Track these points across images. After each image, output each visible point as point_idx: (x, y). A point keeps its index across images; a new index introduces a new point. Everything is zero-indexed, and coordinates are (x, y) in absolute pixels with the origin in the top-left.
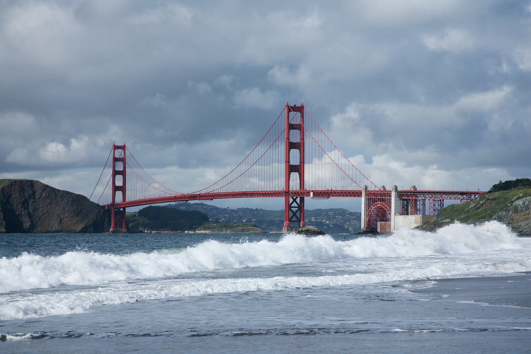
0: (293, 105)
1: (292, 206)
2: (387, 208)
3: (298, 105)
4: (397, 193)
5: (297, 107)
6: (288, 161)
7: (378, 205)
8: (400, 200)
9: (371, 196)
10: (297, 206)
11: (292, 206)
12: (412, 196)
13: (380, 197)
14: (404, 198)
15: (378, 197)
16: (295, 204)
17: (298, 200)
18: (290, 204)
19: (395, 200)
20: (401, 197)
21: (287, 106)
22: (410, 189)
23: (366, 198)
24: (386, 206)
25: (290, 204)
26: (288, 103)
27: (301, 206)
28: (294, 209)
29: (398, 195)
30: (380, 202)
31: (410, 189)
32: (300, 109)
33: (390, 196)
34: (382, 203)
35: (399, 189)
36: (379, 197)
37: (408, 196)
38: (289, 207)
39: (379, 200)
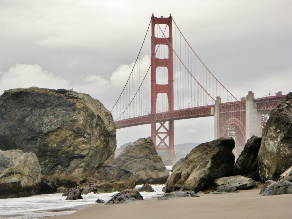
0: (159, 17)
1: (159, 131)
2: (242, 126)
3: (166, 16)
4: (252, 103)
5: (165, 19)
6: (153, 80)
7: (232, 123)
8: (258, 113)
9: (224, 111)
10: (166, 131)
11: (159, 131)
12: (272, 104)
13: (233, 111)
14: (263, 109)
15: (231, 111)
16: (162, 130)
17: (167, 124)
18: (157, 129)
19: (251, 113)
20: (259, 109)
21: (153, 17)
22: (270, 94)
23: (218, 114)
24: (241, 123)
25: (157, 129)
26: (153, 14)
27: (170, 132)
28: (162, 136)
29: (254, 106)
30: (234, 118)
31: (270, 94)
32: (168, 21)
33: (245, 108)
34: (236, 119)
35: (257, 96)
36: (232, 110)
37: (268, 105)
38: (155, 132)
39: (233, 115)
